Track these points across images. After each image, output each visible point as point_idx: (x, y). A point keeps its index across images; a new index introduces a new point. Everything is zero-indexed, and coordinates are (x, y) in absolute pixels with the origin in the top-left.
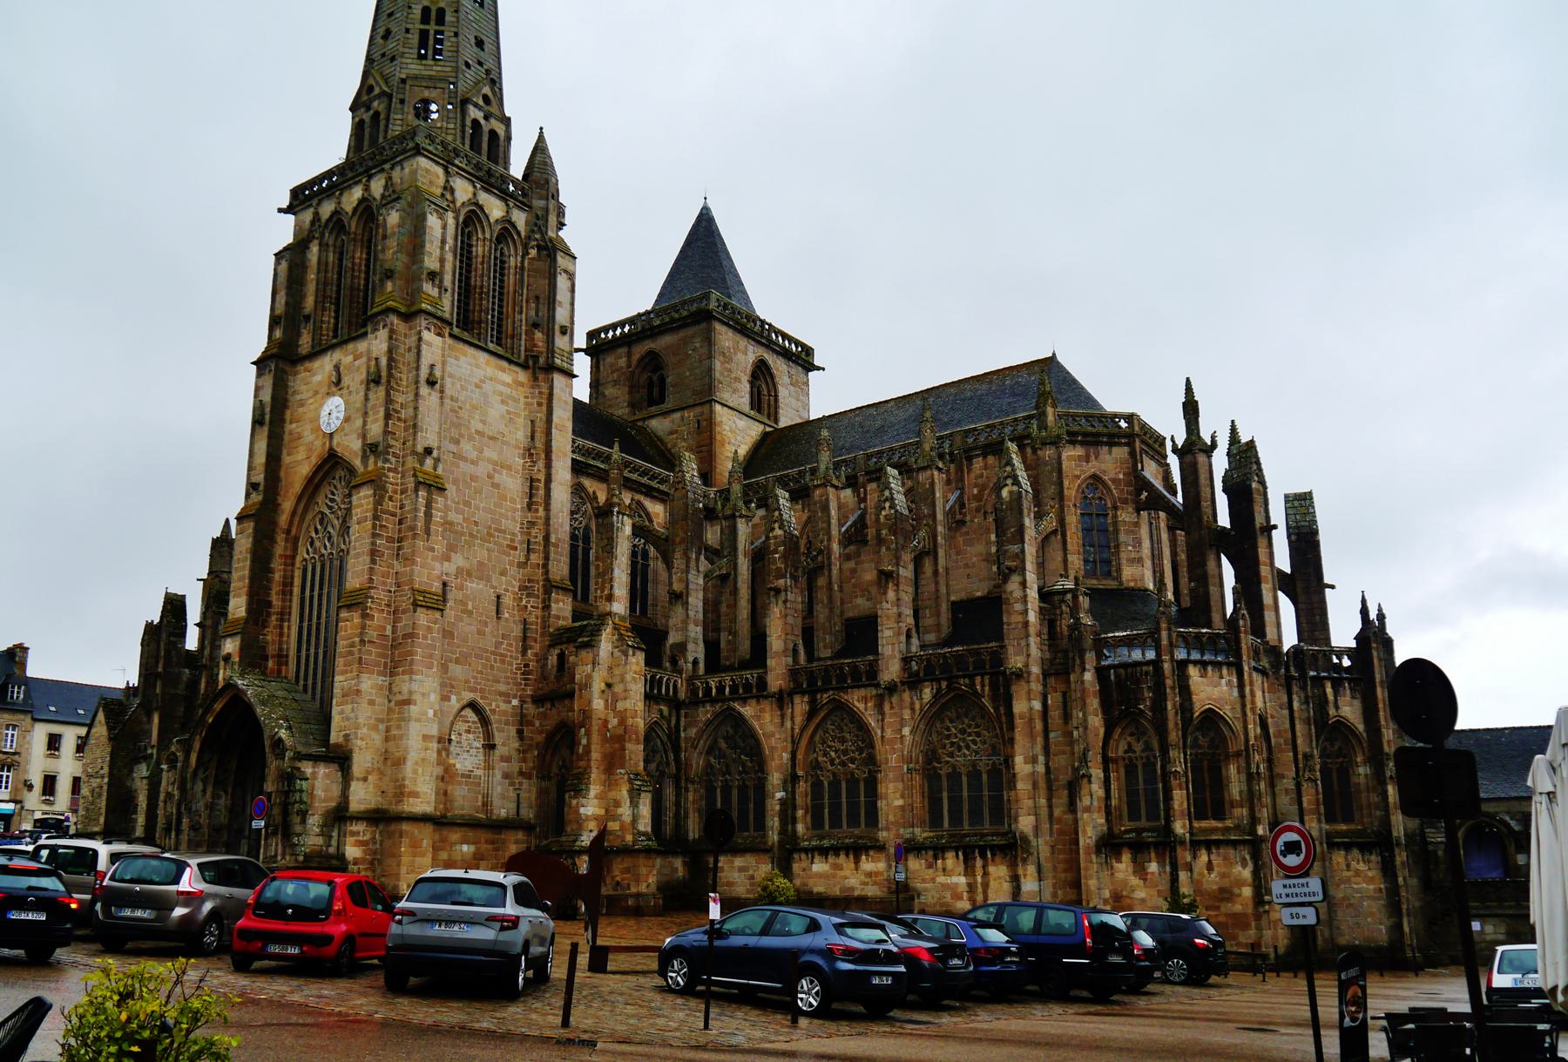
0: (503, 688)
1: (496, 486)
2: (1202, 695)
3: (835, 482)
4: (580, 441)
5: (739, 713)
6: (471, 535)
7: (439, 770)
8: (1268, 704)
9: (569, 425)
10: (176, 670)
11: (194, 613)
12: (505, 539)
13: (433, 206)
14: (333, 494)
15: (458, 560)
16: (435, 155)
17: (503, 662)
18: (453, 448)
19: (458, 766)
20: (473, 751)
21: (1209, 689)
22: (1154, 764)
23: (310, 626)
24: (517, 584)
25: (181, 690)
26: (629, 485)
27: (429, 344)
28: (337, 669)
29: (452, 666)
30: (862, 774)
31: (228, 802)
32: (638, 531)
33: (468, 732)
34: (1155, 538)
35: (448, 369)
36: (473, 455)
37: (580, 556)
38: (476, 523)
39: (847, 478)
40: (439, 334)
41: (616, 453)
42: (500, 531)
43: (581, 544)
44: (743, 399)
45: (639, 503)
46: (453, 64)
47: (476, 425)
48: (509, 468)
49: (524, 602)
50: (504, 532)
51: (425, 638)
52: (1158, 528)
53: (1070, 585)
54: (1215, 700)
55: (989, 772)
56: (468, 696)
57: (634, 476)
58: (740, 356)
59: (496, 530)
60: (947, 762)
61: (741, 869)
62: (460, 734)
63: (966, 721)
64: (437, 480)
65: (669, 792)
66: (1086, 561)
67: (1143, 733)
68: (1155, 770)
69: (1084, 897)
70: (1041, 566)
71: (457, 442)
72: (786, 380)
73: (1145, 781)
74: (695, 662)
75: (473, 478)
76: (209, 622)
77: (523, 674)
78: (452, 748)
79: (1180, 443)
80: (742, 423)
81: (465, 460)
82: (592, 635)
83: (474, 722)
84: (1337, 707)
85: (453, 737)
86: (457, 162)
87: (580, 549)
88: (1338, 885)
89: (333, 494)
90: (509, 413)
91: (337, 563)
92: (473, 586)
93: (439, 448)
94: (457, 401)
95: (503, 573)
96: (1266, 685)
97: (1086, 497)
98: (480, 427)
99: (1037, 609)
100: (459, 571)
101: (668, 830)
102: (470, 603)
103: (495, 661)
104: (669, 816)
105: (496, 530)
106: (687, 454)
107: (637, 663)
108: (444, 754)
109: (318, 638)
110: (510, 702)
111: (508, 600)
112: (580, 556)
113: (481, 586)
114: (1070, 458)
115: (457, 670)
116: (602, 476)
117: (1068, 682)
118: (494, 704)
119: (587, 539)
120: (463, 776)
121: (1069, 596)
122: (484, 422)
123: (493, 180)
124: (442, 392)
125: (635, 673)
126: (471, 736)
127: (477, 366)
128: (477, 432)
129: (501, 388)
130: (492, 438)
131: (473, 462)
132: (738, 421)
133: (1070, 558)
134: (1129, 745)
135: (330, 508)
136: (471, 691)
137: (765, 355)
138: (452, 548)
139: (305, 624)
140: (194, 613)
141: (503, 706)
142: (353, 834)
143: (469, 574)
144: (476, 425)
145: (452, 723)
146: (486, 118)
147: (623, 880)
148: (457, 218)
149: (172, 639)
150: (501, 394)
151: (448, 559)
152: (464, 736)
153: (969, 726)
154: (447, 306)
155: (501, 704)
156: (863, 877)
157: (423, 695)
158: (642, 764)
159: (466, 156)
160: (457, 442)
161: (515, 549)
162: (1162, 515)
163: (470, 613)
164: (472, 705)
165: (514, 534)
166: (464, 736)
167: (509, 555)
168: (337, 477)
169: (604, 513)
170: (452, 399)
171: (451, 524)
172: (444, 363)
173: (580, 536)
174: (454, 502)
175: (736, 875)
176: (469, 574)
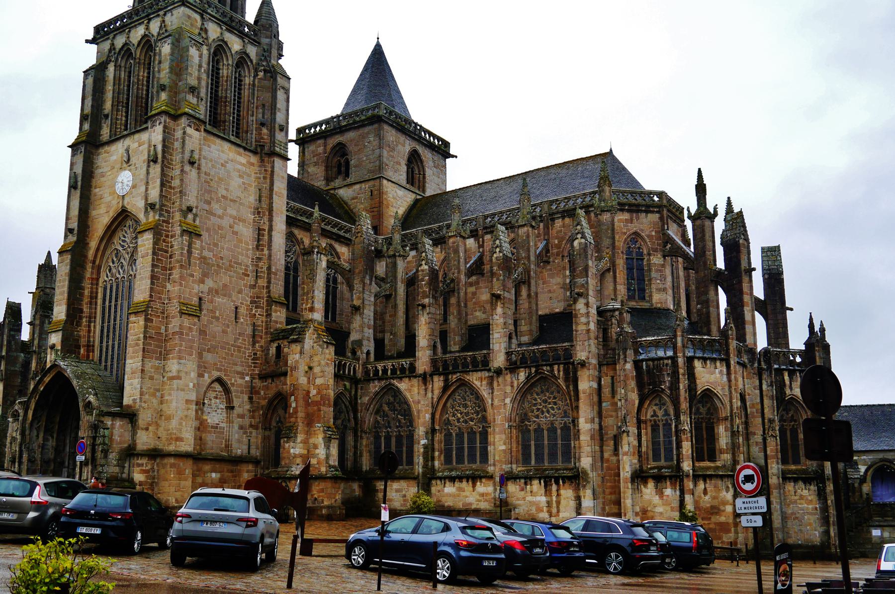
0: (239, 369)
1: (236, 233)
2: (703, 380)
3: (463, 234)
4: (292, 203)
5: (397, 387)
7: (196, 424)
8: (746, 386)
9: (285, 193)
10: (15, 354)
11: (27, 315)
12: (241, 269)
14: (124, 237)
15: (210, 283)
16: (195, 6)
17: (239, 351)
18: (206, 207)
19: (209, 421)
20: (219, 411)
22: (670, 425)
23: (109, 326)
25: (18, 368)
26: (325, 234)
27: (191, 136)
28: (128, 356)
30: (478, 428)
32: (330, 265)
33: (216, 398)
34: (675, 275)
35: (203, 153)
37: (291, 281)
38: (222, 258)
39: (471, 231)
40: (197, 130)
41: (316, 212)
43: (292, 273)
44: (402, 177)
45: (331, 246)
48: (244, 221)
49: (254, 312)
50: (240, 264)
51: (187, 335)
52: (677, 269)
53: (618, 306)
54: (711, 383)
55: (562, 429)
56: (216, 374)
57: (328, 228)
58: (400, 147)
59: (235, 263)
60: (535, 422)
61: (397, 491)
62: (210, 400)
63: (547, 394)
65: (350, 439)
66: (629, 289)
67: (664, 404)
68: (671, 429)
69: (622, 511)
70: (600, 292)
71: (209, 203)
72: (431, 164)
73: (664, 435)
74: (368, 353)
75: (220, 228)
76: (37, 322)
77: (253, 360)
79: (693, 212)
80: (401, 192)
81: (214, 215)
82: (300, 334)
83: (219, 392)
84: (791, 388)
85: (206, 401)
86: (209, 11)
87: (291, 277)
88: (789, 505)
89: (124, 237)
90: (244, 183)
91: (127, 284)
92: (219, 300)
93: (197, 207)
94: (209, 175)
95: (240, 292)
97: (629, 247)
98: (224, 193)
99: (596, 321)
100: (210, 290)
101: (349, 464)
102: (217, 312)
103: (234, 351)
104: (350, 455)
105: (235, 263)
107: (330, 354)
109: (114, 334)
110: (244, 378)
111: (243, 310)
112: (291, 281)
114: (620, 221)
115: (209, 357)
116: (307, 228)
118: (233, 380)
119: (296, 270)
120: (212, 427)
121: (617, 313)
122: (227, 190)
123: (234, 24)
124: (199, 169)
125: (328, 360)
126: (218, 401)
127: (223, 152)
128: (223, 197)
129: (240, 167)
130: (231, 200)
131: (219, 217)
132: (398, 191)
133: (618, 287)
134: (654, 411)
135: (123, 246)
136: (218, 371)
137: (417, 147)
138: (205, 275)
139: (106, 325)
140: (27, 315)
141: (240, 381)
142: (139, 465)
143: (217, 292)
145: (205, 392)
147: (319, 497)
148: (209, 50)
149: (12, 333)
150: (239, 171)
151: (203, 282)
152: (213, 401)
153: (549, 398)
154: (202, 111)
156: (478, 497)
157: (186, 373)
158: (332, 420)
159: (216, 7)
160: (209, 203)
161: (248, 275)
162: (680, 259)
163: (217, 319)
164: (219, 380)
165: (247, 266)
166: (213, 401)
169: (308, 252)
170: (206, 174)
171: (205, 258)
172: (200, 150)
173: (292, 267)
174: (207, 244)
175: (394, 494)
176: (217, 292)
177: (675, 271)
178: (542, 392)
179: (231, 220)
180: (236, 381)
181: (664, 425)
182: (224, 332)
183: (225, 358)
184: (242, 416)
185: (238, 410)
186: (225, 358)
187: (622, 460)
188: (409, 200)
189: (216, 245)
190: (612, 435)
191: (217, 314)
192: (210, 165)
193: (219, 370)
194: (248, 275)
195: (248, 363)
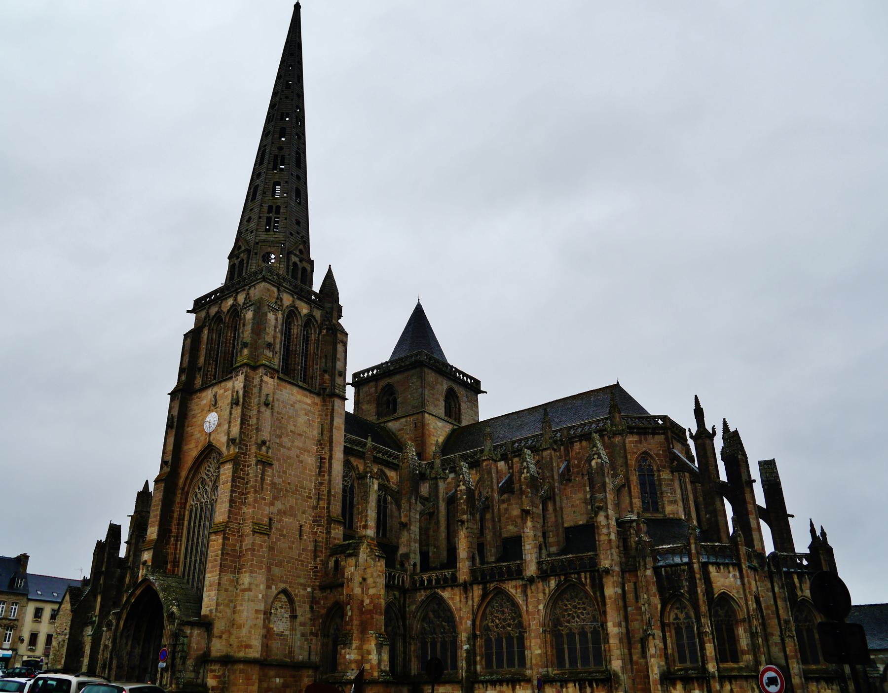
0: (302, 581)
2: (719, 584)
3: (494, 457)
4: (349, 436)
5: (441, 596)
6: (286, 490)
7: (262, 632)
9: (343, 427)
11: (125, 536)
12: (306, 492)
13: (271, 309)
14: (209, 467)
15: (279, 505)
16: (273, 281)
17: (302, 565)
18: (278, 440)
19: (275, 629)
20: (284, 620)
21: (722, 580)
22: (693, 627)
24: (311, 519)
26: (376, 460)
27: (267, 383)
28: (207, 570)
29: (273, 568)
31: (140, 651)
32: (381, 487)
33: (281, 608)
34: (683, 488)
35: (276, 396)
36: (289, 444)
37: (348, 502)
38: (289, 484)
39: (502, 455)
40: (272, 378)
41: (369, 442)
42: (302, 488)
43: (348, 495)
44: (441, 411)
45: (382, 471)
46: (284, 234)
47: (291, 427)
48: (309, 451)
50: (305, 489)
51: (258, 551)
54: (726, 587)
56: (282, 586)
57: (379, 455)
58: (439, 386)
60: (566, 626)
63: (577, 600)
64: (268, 459)
65: (400, 645)
66: (643, 503)
67: (685, 608)
68: (693, 631)
70: (617, 505)
71: (280, 437)
72: (465, 399)
73: (687, 637)
74: (415, 565)
75: (289, 458)
76: (133, 541)
77: (314, 572)
78: (272, 618)
79: (694, 432)
80: (440, 424)
81: (284, 447)
82: (354, 549)
83: (285, 602)
84: (802, 590)
85: (273, 611)
86: (284, 284)
87: (348, 498)
89: (209, 467)
90: (309, 420)
91: (209, 507)
92: (286, 520)
93: (269, 441)
95: (304, 512)
96: (757, 577)
97: (641, 465)
98: (293, 428)
99: (615, 531)
100: (279, 511)
101: (399, 669)
102: (285, 530)
103: (298, 565)
104: (400, 659)
105: (302, 488)
106: (409, 442)
107: (381, 566)
108: (267, 621)
109: (196, 551)
110: (306, 590)
111: (306, 529)
112: (348, 502)
113: (291, 520)
114: (631, 442)
115: (276, 570)
116: (361, 456)
117: (637, 576)
118: (297, 591)
120: (278, 635)
121: (634, 524)
122: (295, 426)
123: (303, 294)
124: (272, 409)
125: (380, 571)
126: (283, 610)
127: (292, 394)
128: (292, 431)
129: (306, 407)
130: (300, 435)
131: (289, 449)
132: (438, 423)
134: (676, 614)
135: (207, 475)
136: (284, 583)
138: (275, 498)
139: (190, 543)
140: (125, 536)
141: (302, 592)
142: (212, 671)
143: (285, 513)
144: (291, 427)
145: (273, 602)
146: (300, 261)
148: (283, 314)
149: (112, 551)
150: (305, 410)
151: (272, 504)
153: (579, 604)
154: (276, 362)
155: (301, 591)
159: (290, 281)
160: (280, 437)
161: (311, 498)
162: (687, 474)
163: (284, 536)
165: (310, 490)
166: (279, 611)
167: (307, 502)
168: (212, 457)
169: (362, 477)
170: (278, 413)
172: (274, 393)
173: (348, 490)
176: (285, 513)
177: (683, 484)
178: (572, 598)
179: (298, 451)
180: (299, 592)
181: (686, 628)
182: (290, 548)
183: (290, 572)
184: (303, 624)
185: (300, 619)
186: (290, 572)
187: (650, 662)
188: (447, 430)
189: (284, 472)
190: (639, 639)
191: (285, 533)
192: (282, 406)
193: (285, 582)
194: (311, 498)
195: (310, 575)
